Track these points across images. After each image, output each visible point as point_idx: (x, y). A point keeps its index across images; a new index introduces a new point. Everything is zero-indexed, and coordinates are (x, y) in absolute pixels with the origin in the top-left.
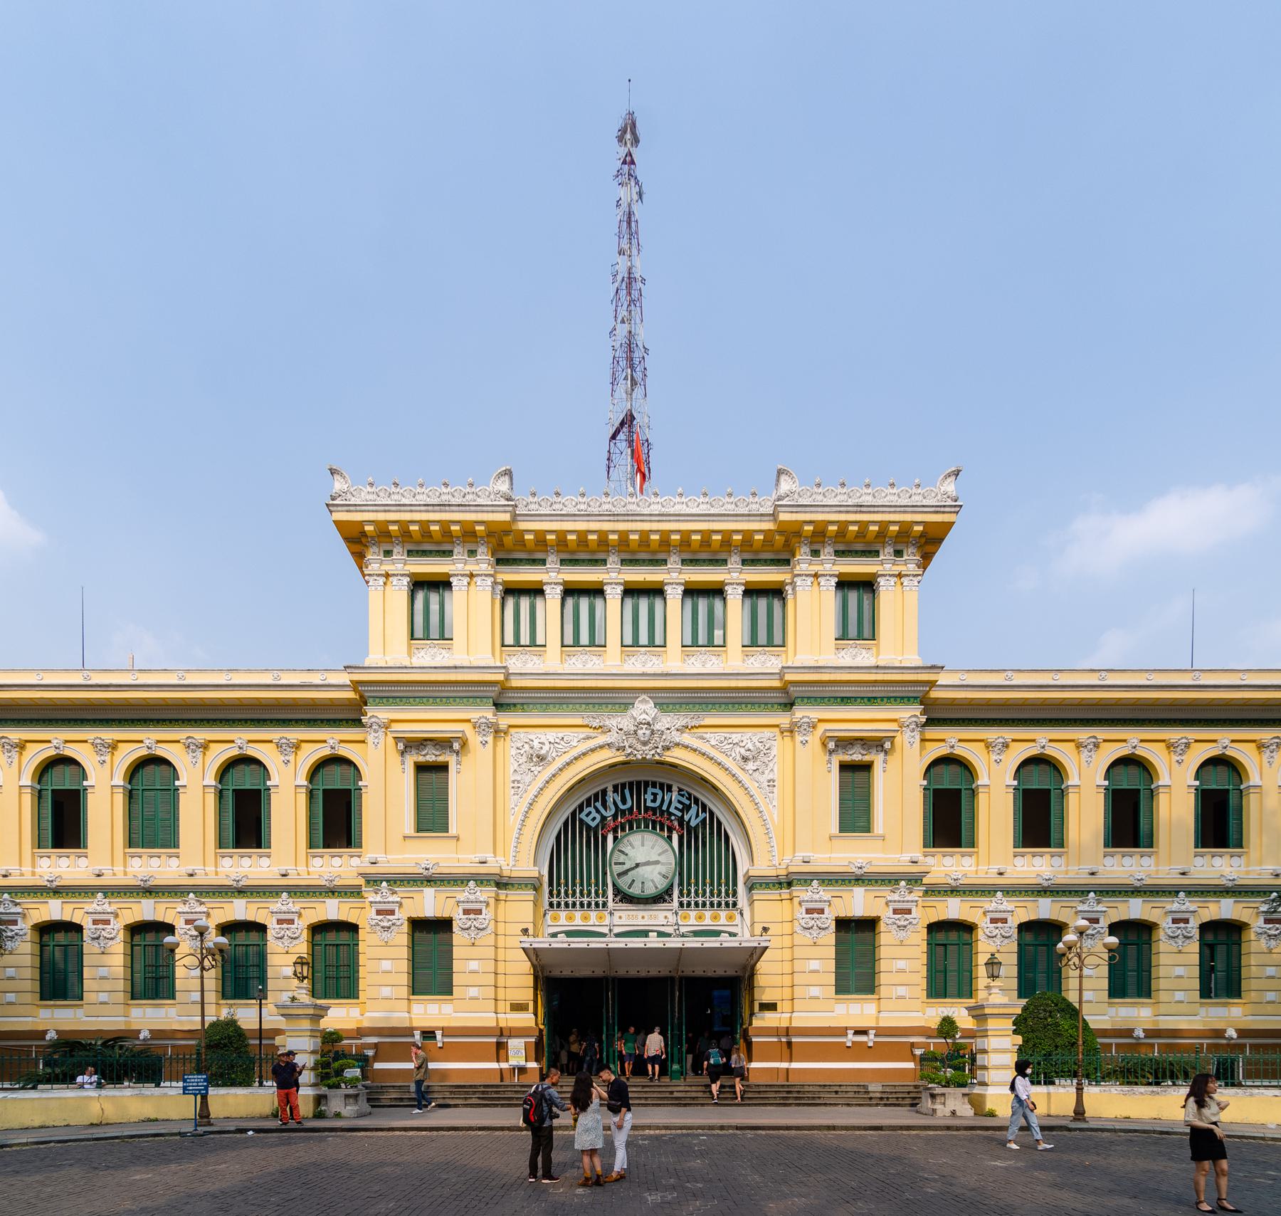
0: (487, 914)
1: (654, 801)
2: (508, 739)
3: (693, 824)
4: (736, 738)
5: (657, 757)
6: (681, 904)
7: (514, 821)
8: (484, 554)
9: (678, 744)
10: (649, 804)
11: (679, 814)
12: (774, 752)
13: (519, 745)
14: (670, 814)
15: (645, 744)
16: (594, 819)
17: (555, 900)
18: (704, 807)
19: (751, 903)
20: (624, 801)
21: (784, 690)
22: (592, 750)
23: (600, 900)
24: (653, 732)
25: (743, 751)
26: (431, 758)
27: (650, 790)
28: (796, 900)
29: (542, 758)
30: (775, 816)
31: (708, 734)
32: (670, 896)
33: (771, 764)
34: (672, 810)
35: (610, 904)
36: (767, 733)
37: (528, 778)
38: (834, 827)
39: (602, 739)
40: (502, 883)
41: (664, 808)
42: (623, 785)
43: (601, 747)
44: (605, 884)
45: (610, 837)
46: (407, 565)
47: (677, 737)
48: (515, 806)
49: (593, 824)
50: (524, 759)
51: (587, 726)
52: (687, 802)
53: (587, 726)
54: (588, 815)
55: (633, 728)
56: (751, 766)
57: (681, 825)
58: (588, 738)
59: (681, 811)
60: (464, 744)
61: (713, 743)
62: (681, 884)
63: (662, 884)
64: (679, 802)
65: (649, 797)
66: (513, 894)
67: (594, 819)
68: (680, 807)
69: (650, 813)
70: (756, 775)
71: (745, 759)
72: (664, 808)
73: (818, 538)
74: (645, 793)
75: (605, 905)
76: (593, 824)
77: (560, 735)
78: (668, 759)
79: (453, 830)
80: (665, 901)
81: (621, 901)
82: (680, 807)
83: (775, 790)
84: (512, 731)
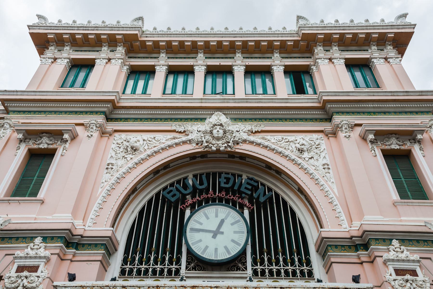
0: (44, 271)
1: (227, 183)
2: (111, 138)
3: (262, 199)
4: (291, 137)
5: (229, 149)
6: (255, 273)
7: (101, 192)
8: (121, 50)
9: (245, 141)
10: (223, 185)
11: (249, 193)
12: (323, 147)
13: (119, 142)
14: (241, 193)
15: (218, 139)
16: (174, 195)
17: (128, 267)
18: (270, 190)
19: (328, 268)
20: (201, 183)
21: (323, 108)
22: (177, 144)
23: (174, 267)
24: (225, 132)
25: (298, 146)
26: (43, 146)
27: (223, 175)
28: (379, 261)
29: (135, 150)
30: (336, 190)
31: (268, 136)
32: (244, 263)
33: (323, 155)
34: (242, 189)
35: (183, 271)
36: (315, 136)
37: (121, 162)
38: (395, 196)
39: (184, 138)
40: (71, 242)
41: (236, 188)
42: (201, 175)
43: (184, 142)
44: (180, 252)
45: (188, 212)
46: (69, 53)
47: (245, 136)
48: (107, 179)
49: (173, 200)
50: (122, 149)
51: (174, 131)
52: (256, 184)
53: (174, 131)
54: (168, 193)
55: (209, 129)
56: (306, 155)
57: (251, 202)
58: (174, 138)
59: (251, 190)
60: (74, 137)
61: (273, 141)
62: (254, 252)
63: (235, 250)
64: (248, 183)
65: (223, 180)
66: (83, 254)
67: (174, 195)
68: (250, 187)
69: (224, 193)
70: (312, 161)
71: (301, 151)
72: (236, 188)
73: (328, 41)
74: (220, 177)
75: (177, 272)
76: (173, 200)
77: (152, 137)
78: (237, 150)
79: (41, 195)
80: (238, 269)
81: (194, 269)
82: (250, 187)
83: (330, 171)
84: (117, 134)
